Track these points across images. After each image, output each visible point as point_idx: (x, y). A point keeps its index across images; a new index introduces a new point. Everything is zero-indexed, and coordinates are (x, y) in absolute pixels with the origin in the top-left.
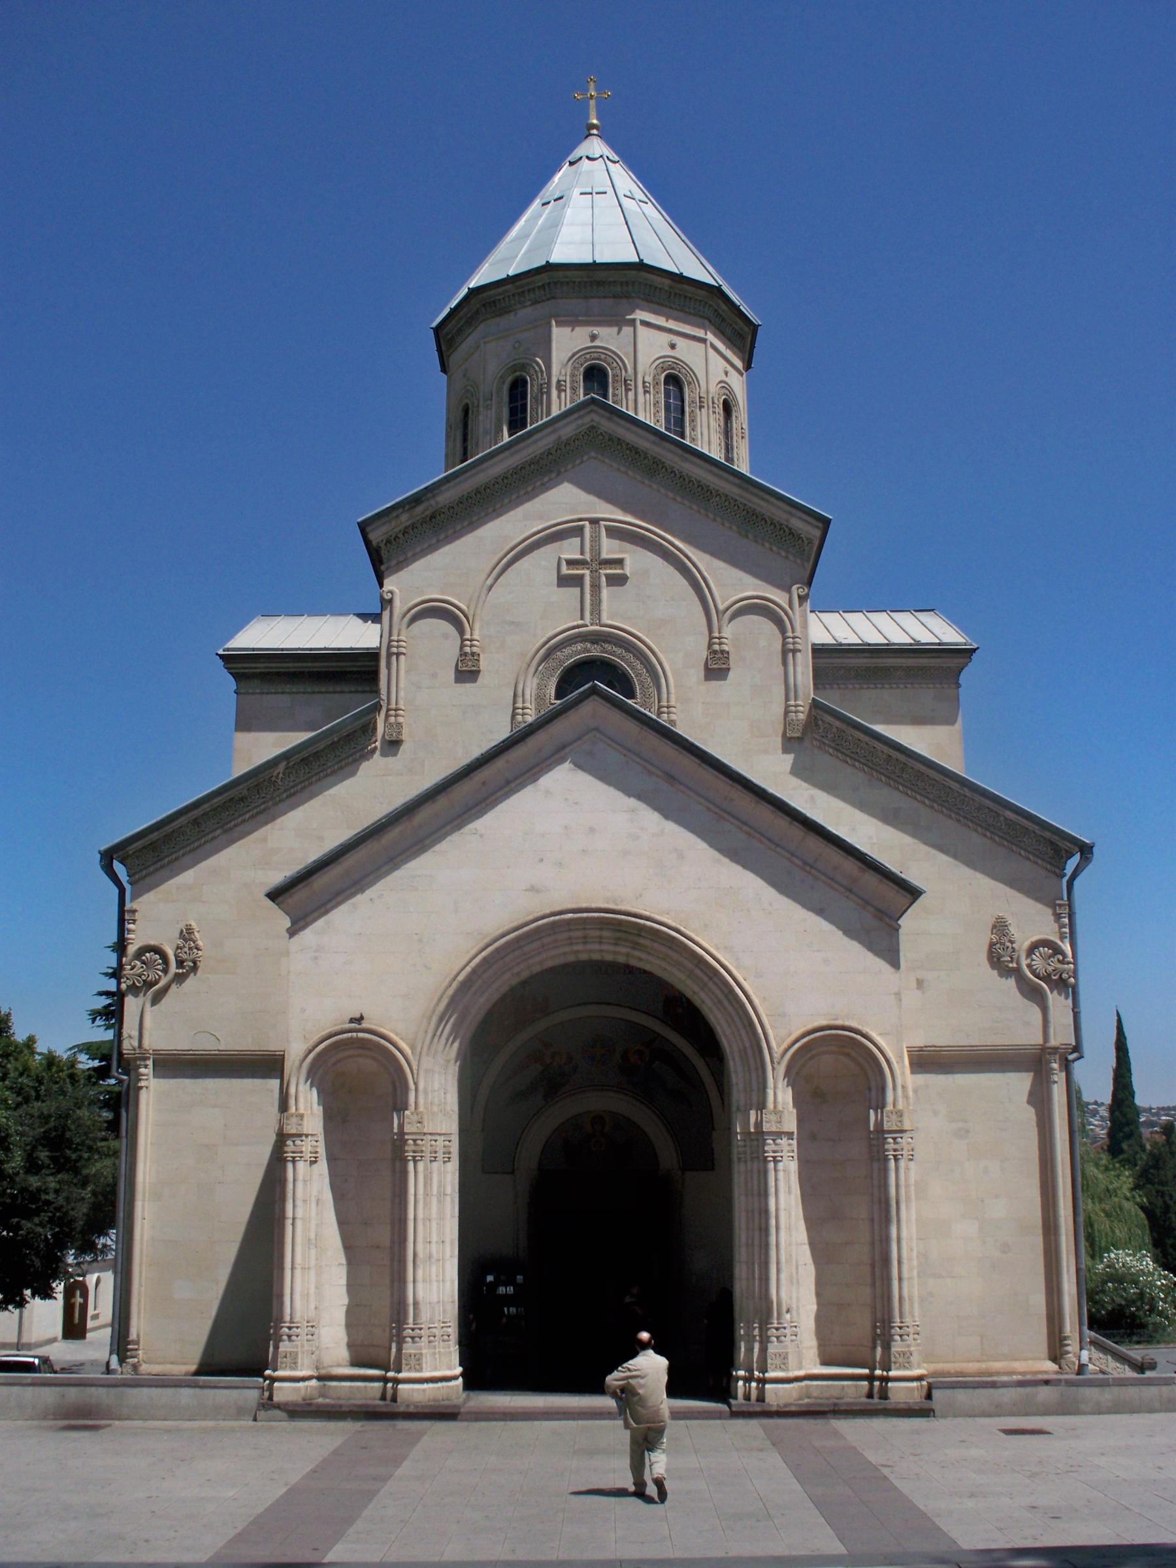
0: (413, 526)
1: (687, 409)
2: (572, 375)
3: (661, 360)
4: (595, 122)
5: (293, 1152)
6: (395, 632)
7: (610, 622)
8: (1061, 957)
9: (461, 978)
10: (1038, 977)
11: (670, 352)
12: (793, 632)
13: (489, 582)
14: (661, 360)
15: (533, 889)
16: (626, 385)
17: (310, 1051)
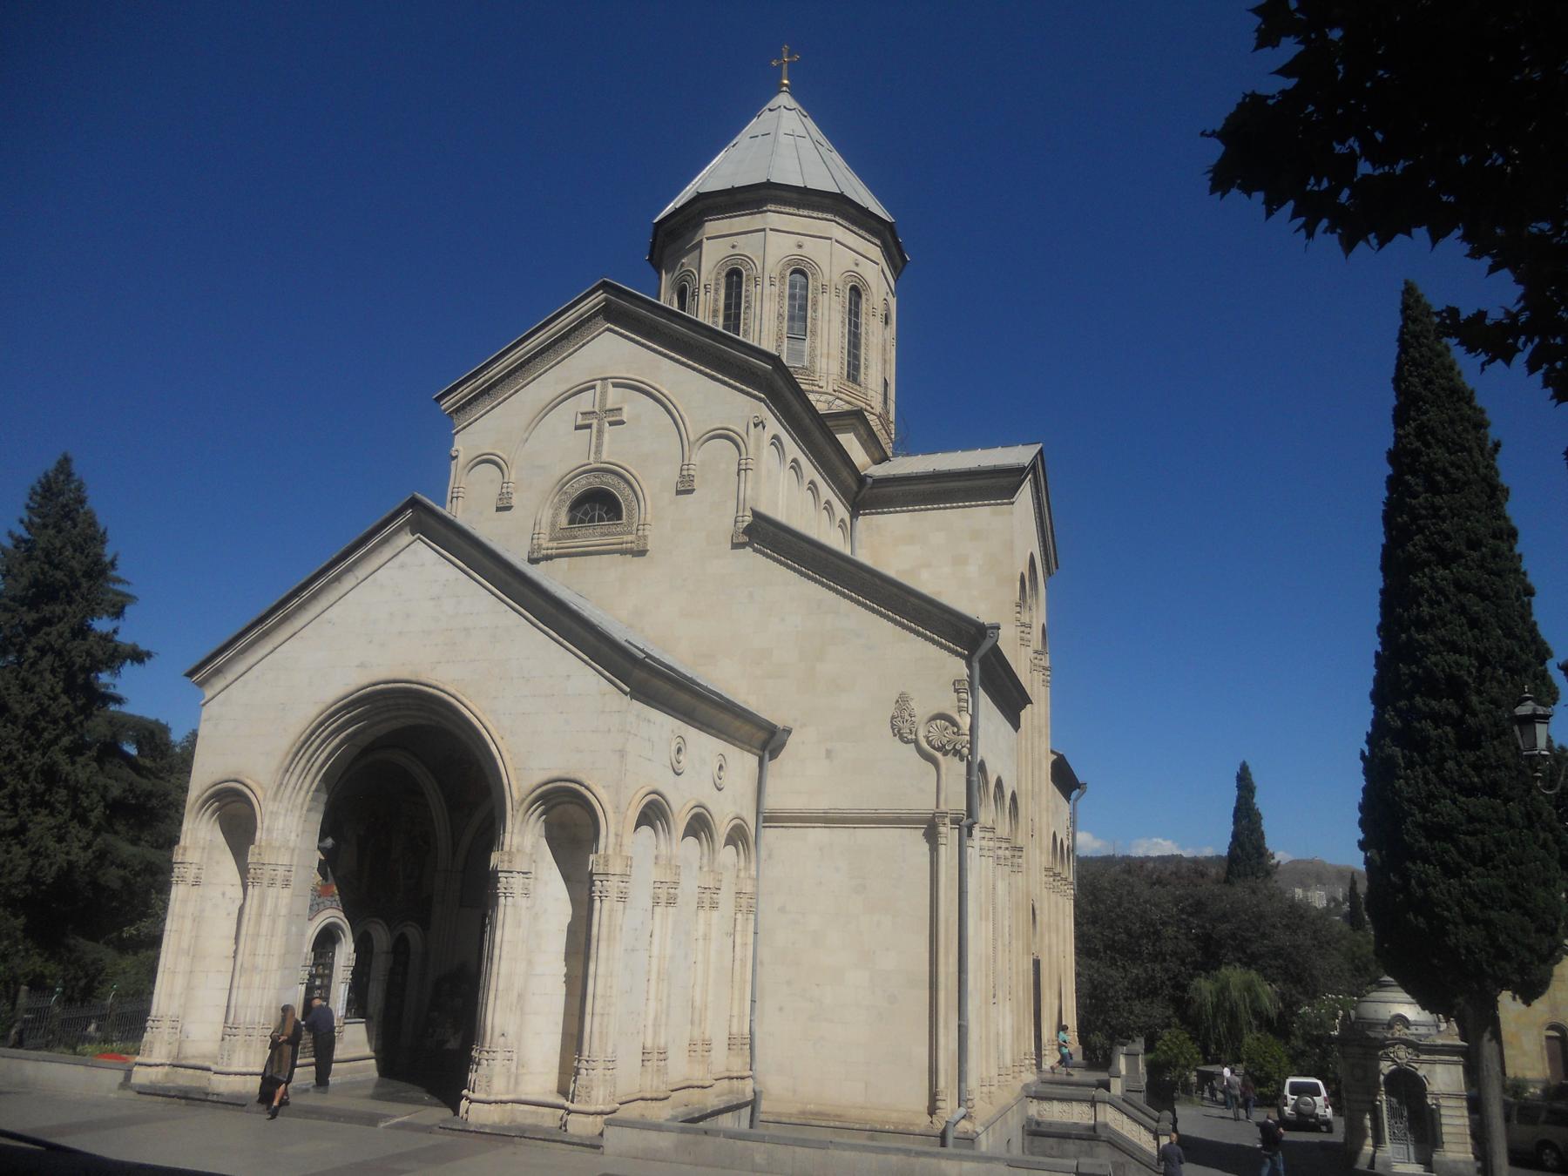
0: (475, 398)
1: (810, 296)
2: (717, 279)
3: (785, 260)
4: (786, 82)
5: (178, 877)
6: (457, 481)
7: (607, 460)
8: (956, 730)
9: (302, 738)
10: (933, 747)
11: (799, 251)
12: (747, 454)
13: (526, 435)
14: (785, 260)
15: (362, 666)
16: (756, 281)
17: (199, 797)
